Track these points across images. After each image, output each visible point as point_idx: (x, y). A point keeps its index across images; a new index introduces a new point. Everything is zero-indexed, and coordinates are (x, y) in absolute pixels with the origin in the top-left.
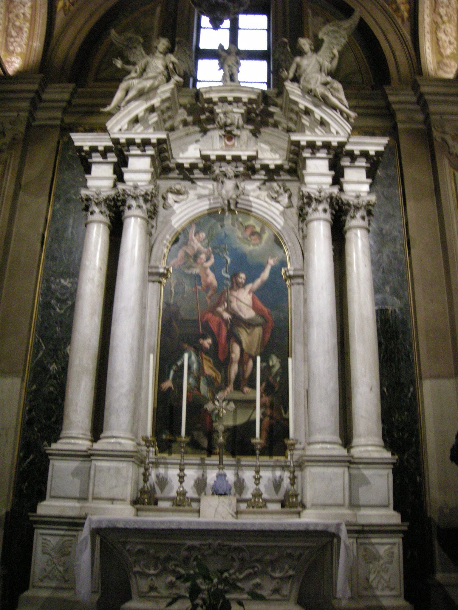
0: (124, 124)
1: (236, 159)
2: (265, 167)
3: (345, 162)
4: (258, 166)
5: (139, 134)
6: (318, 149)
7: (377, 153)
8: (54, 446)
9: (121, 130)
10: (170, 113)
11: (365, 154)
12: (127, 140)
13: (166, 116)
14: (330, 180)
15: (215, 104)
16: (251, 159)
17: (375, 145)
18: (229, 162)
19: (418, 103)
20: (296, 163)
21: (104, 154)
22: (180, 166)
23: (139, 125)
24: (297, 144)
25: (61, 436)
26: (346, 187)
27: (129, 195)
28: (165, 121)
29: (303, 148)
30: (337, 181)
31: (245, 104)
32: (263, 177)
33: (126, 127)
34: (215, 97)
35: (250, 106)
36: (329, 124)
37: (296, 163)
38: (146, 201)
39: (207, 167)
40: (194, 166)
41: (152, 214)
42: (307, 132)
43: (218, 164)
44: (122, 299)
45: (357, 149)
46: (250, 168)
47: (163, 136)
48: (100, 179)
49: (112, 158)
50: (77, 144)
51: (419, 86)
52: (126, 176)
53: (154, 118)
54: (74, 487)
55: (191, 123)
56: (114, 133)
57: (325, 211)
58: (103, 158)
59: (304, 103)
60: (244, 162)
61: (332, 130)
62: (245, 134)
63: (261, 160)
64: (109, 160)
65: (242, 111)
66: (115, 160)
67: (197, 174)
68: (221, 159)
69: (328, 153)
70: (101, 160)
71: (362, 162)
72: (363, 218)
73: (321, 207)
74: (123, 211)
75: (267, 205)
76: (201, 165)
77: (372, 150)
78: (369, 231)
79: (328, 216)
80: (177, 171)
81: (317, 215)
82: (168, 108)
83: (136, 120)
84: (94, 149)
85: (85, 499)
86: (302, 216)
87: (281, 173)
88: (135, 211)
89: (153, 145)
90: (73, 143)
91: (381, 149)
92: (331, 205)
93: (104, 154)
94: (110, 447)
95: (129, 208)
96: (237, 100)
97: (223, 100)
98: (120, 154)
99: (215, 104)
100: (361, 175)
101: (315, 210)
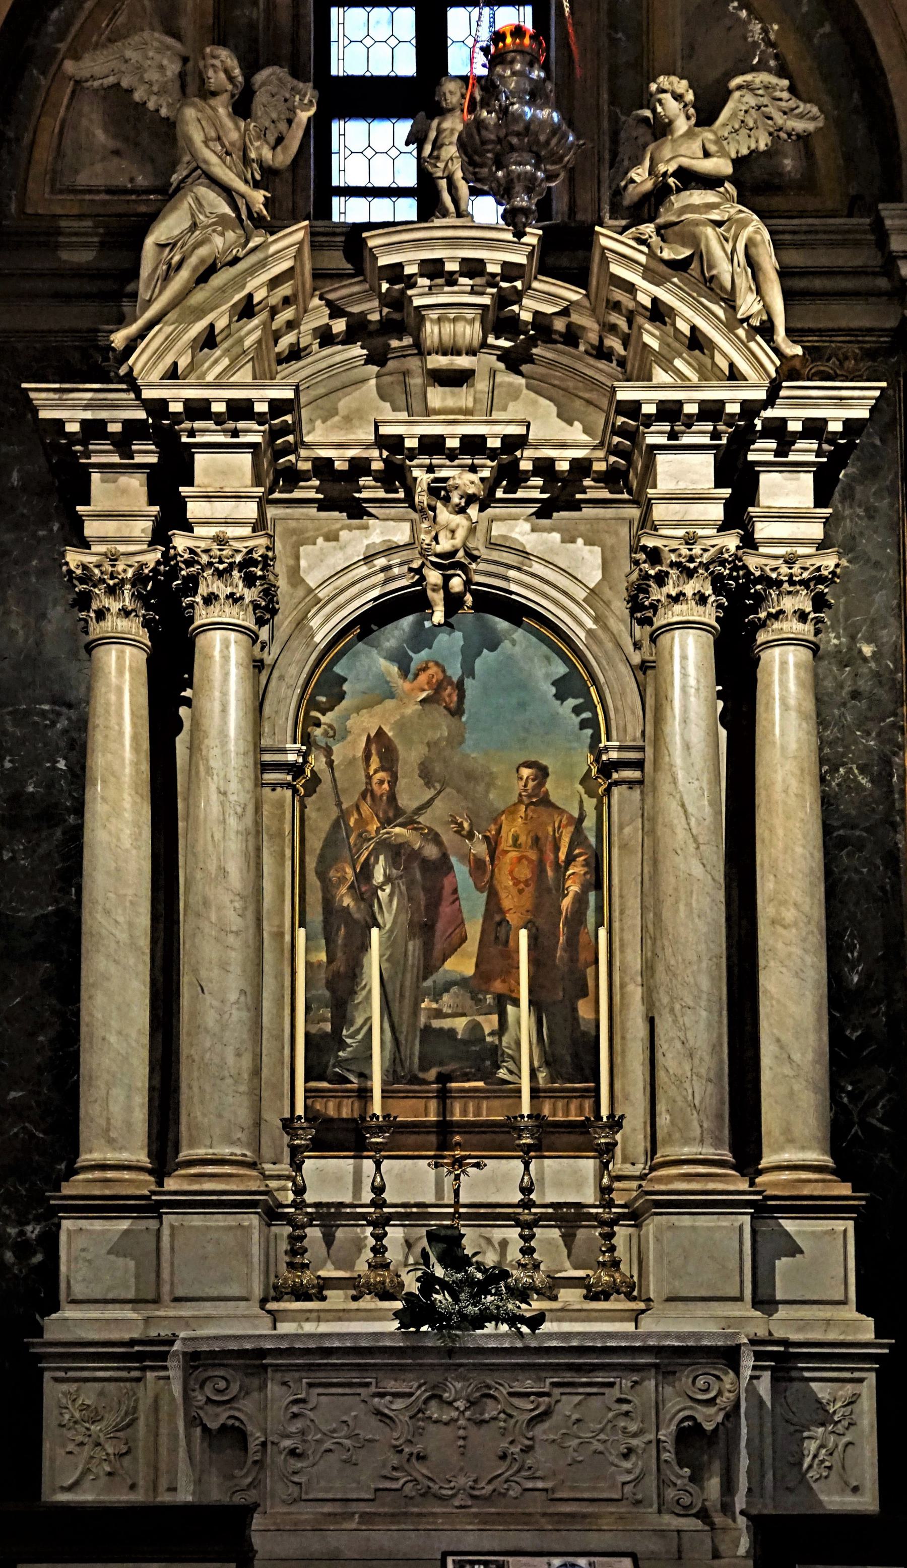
1: (473, 445)
6: (690, 421)
10: (288, 314)
14: (717, 512)
15: (410, 281)
16: (514, 443)
22: (323, 467)
24: (632, 409)
28: (277, 337)
30: (737, 516)
34: (410, 261)
35: (504, 285)
40: (359, 467)
41: (266, 611)
42: (660, 376)
44: (192, 823)
48: (117, 515)
50: (43, 414)
57: (702, 599)
60: (493, 454)
64: (138, 459)
66: (153, 459)
68: (432, 445)
69: (715, 435)
70: (116, 459)
73: (690, 588)
84: (94, 430)
90: (35, 411)
92: (718, 583)
96: (473, 268)
97: (433, 269)
99: (410, 281)
101: (677, 599)
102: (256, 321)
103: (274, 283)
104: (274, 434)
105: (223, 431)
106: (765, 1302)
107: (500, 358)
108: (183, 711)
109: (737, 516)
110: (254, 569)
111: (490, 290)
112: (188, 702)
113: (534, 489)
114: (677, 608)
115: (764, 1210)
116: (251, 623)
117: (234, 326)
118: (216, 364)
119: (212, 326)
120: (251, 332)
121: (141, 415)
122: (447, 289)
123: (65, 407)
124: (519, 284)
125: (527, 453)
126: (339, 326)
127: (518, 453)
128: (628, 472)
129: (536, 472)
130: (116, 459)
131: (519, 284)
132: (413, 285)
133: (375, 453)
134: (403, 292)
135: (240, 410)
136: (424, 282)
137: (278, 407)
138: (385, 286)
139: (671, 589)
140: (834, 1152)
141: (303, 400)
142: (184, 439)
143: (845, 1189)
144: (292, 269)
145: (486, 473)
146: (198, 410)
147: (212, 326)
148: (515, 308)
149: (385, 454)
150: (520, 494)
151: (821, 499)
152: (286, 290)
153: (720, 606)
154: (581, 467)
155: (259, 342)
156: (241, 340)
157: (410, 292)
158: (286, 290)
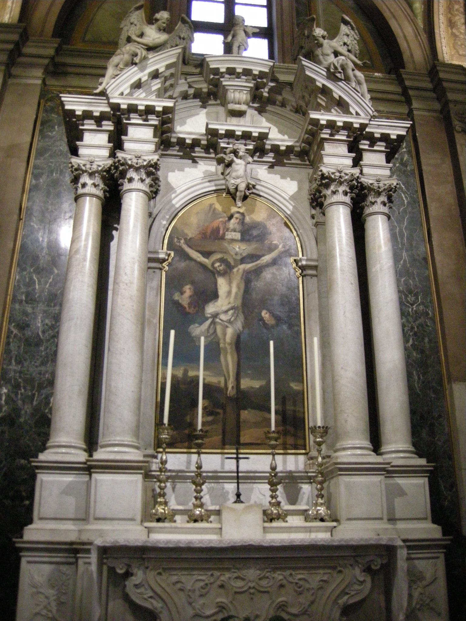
0: (126, 88)
1: (246, 136)
2: (275, 149)
3: (364, 145)
4: (268, 147)
5: (142, 100)
7: (399, 136)
8: (42, 457)
9: (122, 94)
11: (385, 138)
12: (130, 105)
13: (168, 83)
15: (222, 75)
16: (263, 136)
17: (396, 129)
18: (238, 138)
19: (434, 90)
20: (310, 144)
21: (99, 120)
23: (141, 91)
25: (49, 444)
26: (366, 170)
27: (131, 166)
29: (322, 127)
31: (255, 77)
32: (271, 160)
33: (128, 91)
35: (259, 80)
36: (347, 104)
37: (310, 144)
38: (149, 174)
39: (210, 144)
43: (226, 140)
45: (377, 132)
46: (259, 147)
47: (170, 104)
49: (108, 126)
51: (437, 72)
52: (127, 145)
53: (156, 85)
54: (70, 505)
55: (192, 96)
56: (113, 98)
58: (98, 126)
59: (321, 81)
61: (351, 110)
62: (251, 113)
63: (271, 140)
64: (104, 128)
65: (251, 85)
66: (112, 128)
67: (198, 152)
68: (230, 134)
70: (94, 127)
71: (381, 146)
72: (384, 204)
74: (122, 185)
75: (282, 187)
76: (204, 142)
77: (394, 134)
78: (389, 218)
79: (347, 199)
80: (177, 148)
81: (335, 198)
82: (172, 75)
83: (138, 85)
85: (85, 519)
86: (317, 202)
87: (292, 156)
88: (136, 185)
89: (158, 114)
91: (403, 133)
93: (99, 120)
94: (112, 457)
95: (131, 180)
98: (118, 123)
99: (222, 75)
100: (381, 159)
102: (158, 81)
103: (168, 67)
104: (163, 123)
105: (142, 119)
106: (392, 520)
107: (256, 110)
108: (114, 232)
109: (357, 162)
110: (152, 171)
111: (253, 82)
112: (117, 229)
113: (270, 158)
114: (335, 196)
115: (388, 471)
116: (149, 191)
117: (149, 82)
118: (140, 94)
119: (140, 79)
120: (156, 85)
121: (108, 109)
122: (236, 80)
123: (75, 103)
124: (265, 80)
125: (268, 142)
126: (191, 91)
127: (265, 141)
128: (309, 151)
129: (271, 151)
130: (94, 127)
131: (265, 80)
132: (223, 77)
133: (205, 138)
134: (219, 79)
135: (149, 110)
136: (227, 76)
137: (167, 110)
138: (212, 77)
139: (332, 188)
140: (414, 445)
141: (176, 108)
142: (125, 121)
143: (423, 462)
144: (174, 63)
145: (251, 147)
146: (132, 109)
147: (140, 79)
148: (262, 90)
149: (210, 137)
150: (265, 159)
151: (388, 161)
152: (172, 70)
153: (352, 199)
154: (290, 149)
155: (159, 89)
156: (151, 87)
157: (222, 79)
158: (172, 70)
